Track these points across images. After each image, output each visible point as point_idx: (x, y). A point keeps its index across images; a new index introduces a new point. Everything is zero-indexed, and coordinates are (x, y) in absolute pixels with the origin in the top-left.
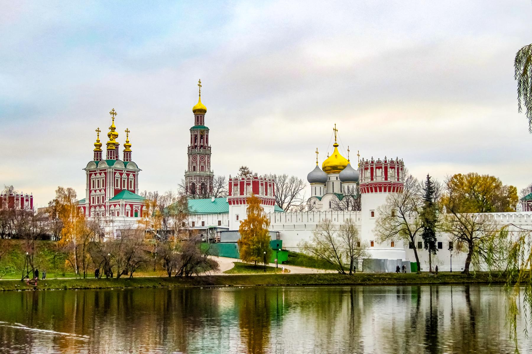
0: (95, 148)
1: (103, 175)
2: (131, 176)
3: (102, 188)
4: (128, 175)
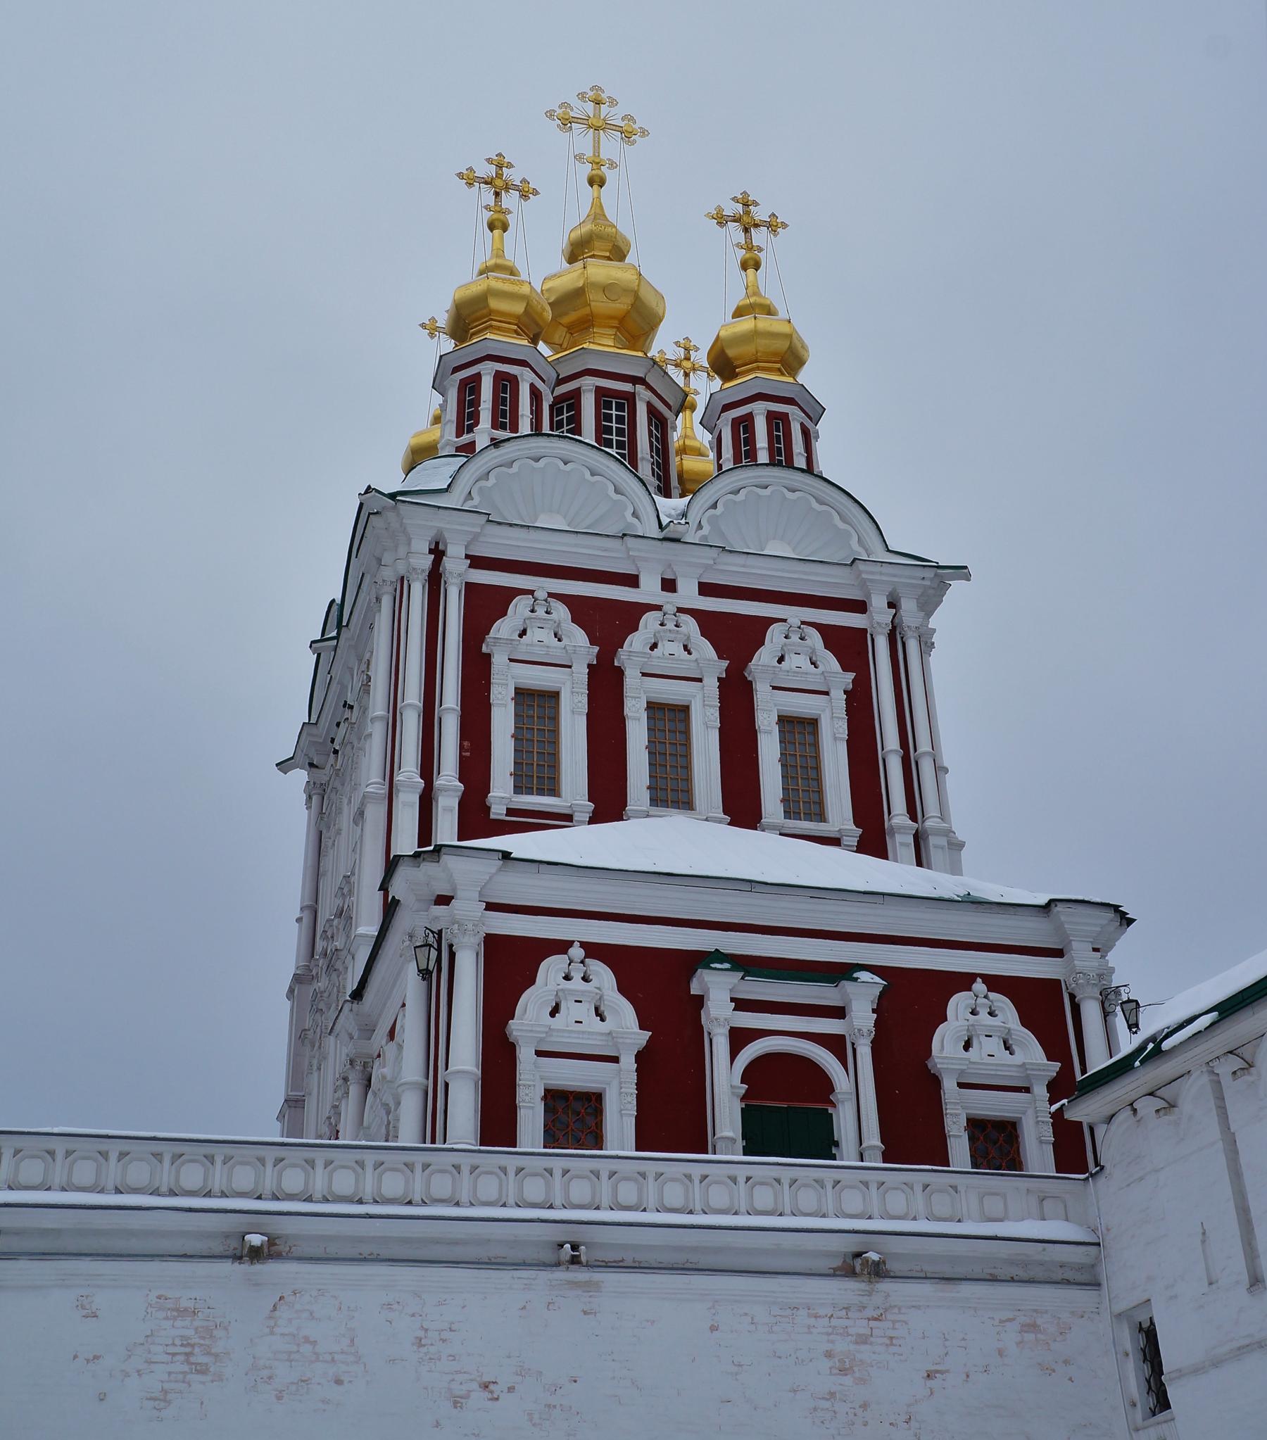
4: (736, 639)
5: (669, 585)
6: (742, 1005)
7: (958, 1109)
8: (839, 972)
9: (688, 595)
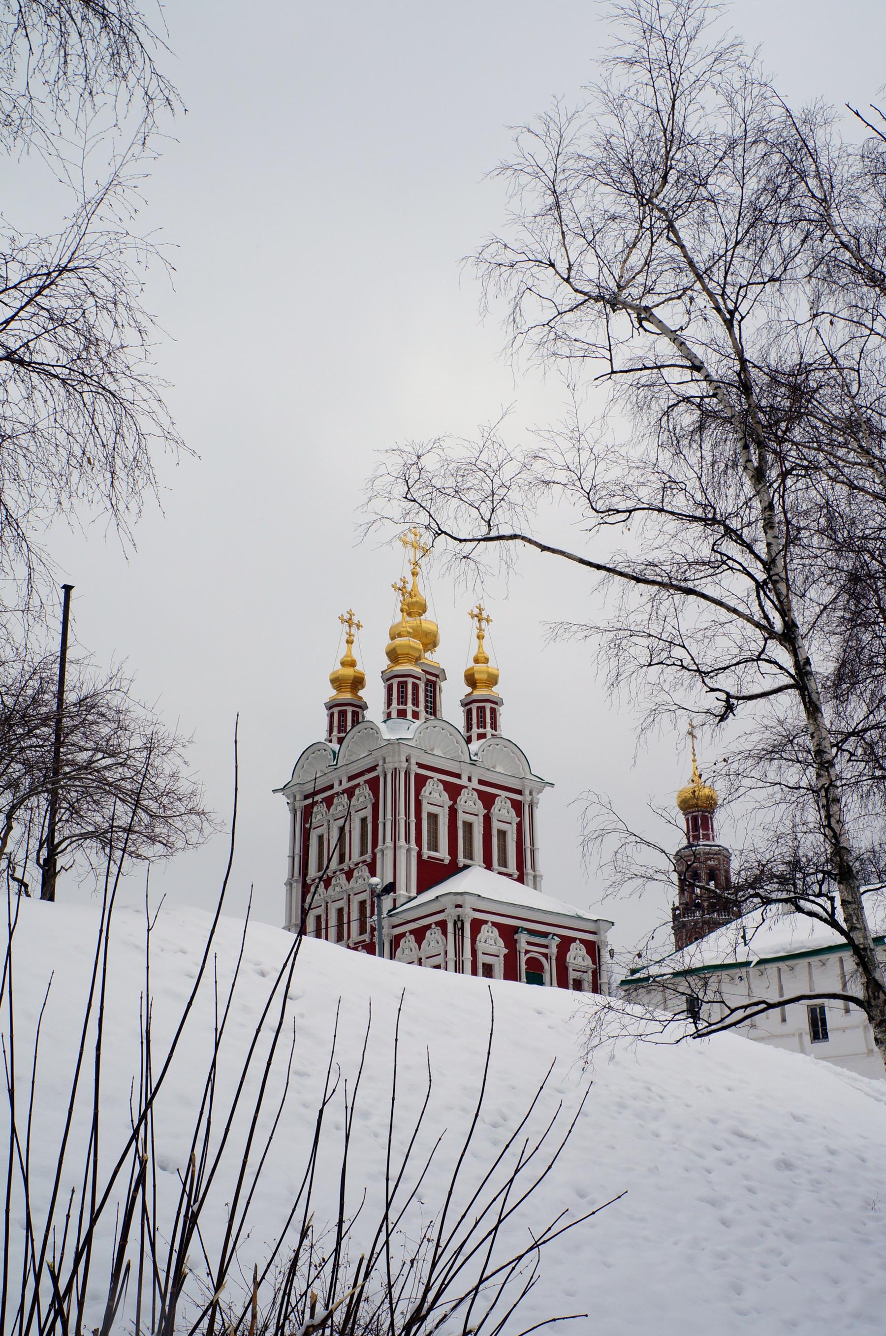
0: (331, 693)
1: (364, 794)
2: (502, 810)
3: (356, 857)
4: (488, 800)
5: (470, 779)
6: (529, 943)
7: (572, 975)
8: (545, 935)
9: (475, 784)
